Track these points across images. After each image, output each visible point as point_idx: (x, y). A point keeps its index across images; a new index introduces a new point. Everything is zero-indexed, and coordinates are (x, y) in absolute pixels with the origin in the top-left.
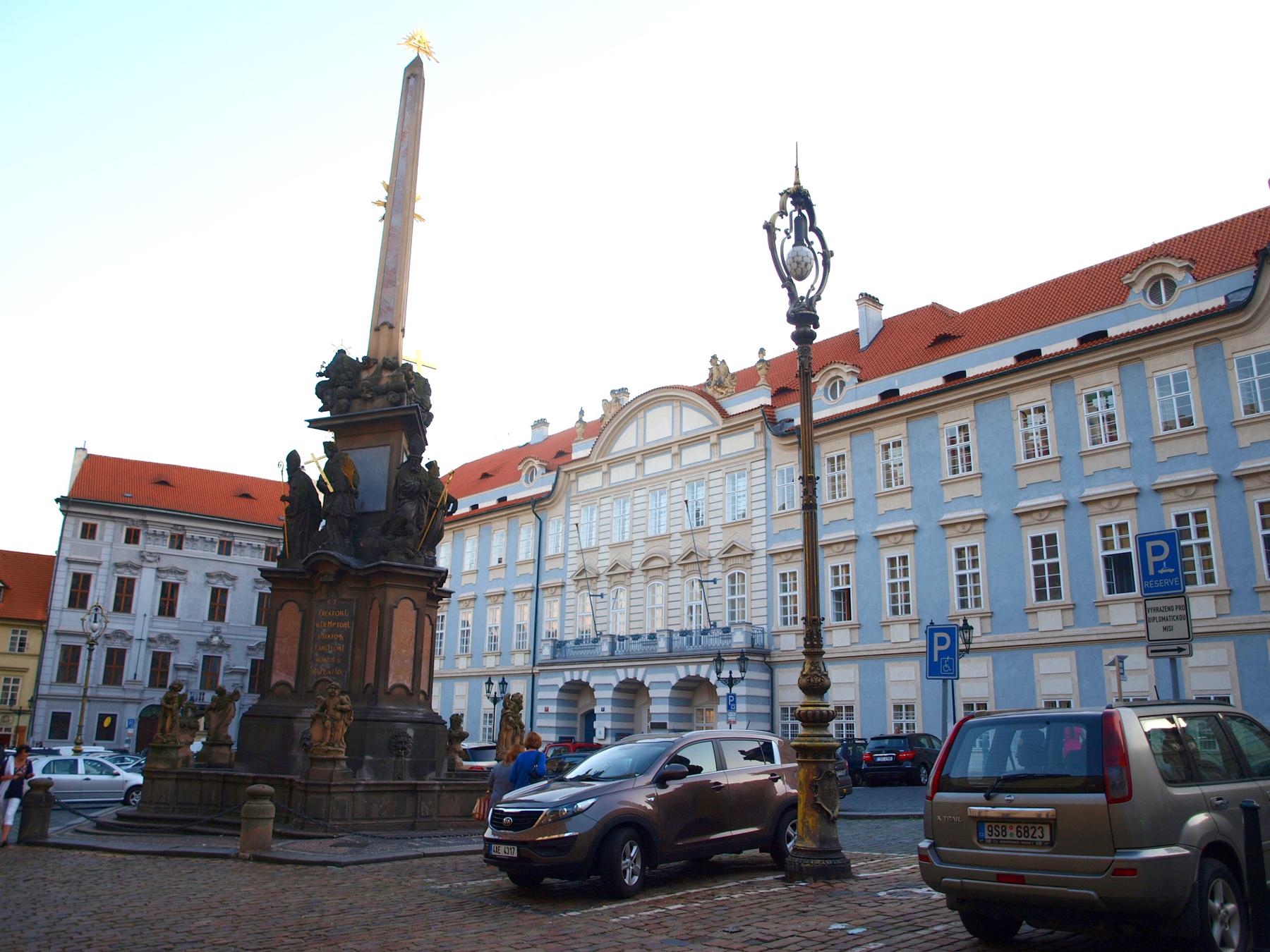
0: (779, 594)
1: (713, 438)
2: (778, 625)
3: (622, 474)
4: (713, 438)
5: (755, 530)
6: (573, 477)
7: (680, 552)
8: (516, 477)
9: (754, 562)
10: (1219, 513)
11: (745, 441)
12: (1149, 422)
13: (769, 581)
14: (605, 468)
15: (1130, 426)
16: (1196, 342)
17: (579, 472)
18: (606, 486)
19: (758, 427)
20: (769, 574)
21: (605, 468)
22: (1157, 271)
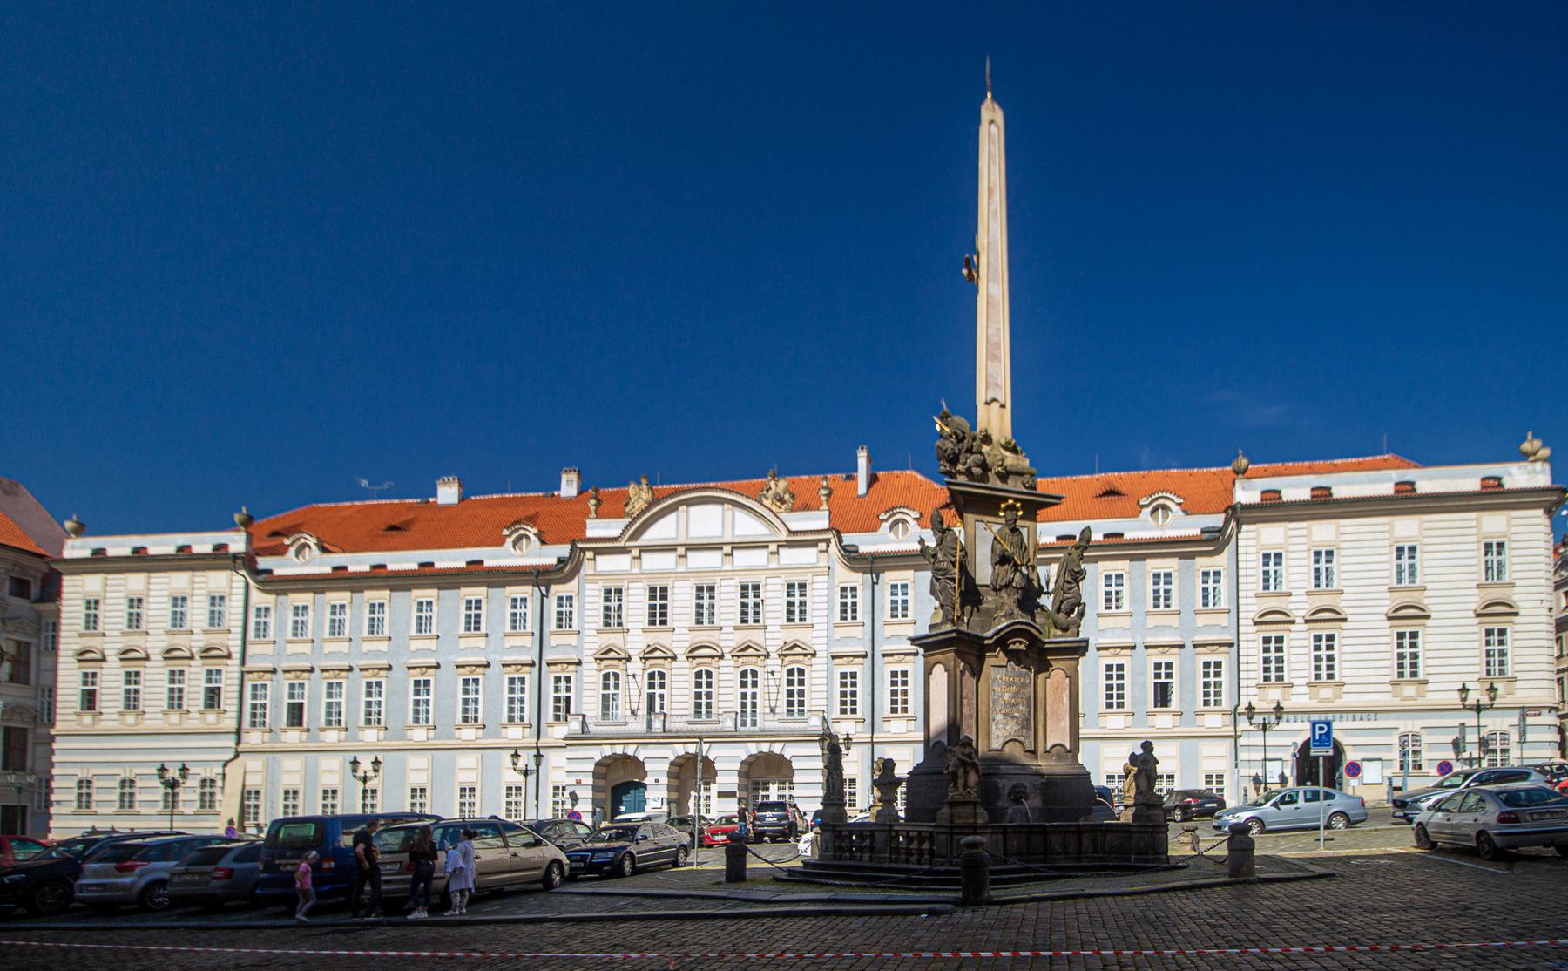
0: (838, 689)
1: (773, 547)
2: (836, 713)
3: (651, 561)
4: (773, 547)
5: (815, 634)
6: (590, 554)
7: (733, 644)
8: (500, 542)
9: (814, 660)
10: (1181, 665)
11: (808, 555)
12: (1144, 601)
13: (829, 678)
14: (635, 552)
15: (1133, 601)
16: (1182, 556)
17: (598, 552)
18: (636, 570)
19: (822, 546)
20: (829, 672)
21: (635, 552)
22: (1161, 501)
